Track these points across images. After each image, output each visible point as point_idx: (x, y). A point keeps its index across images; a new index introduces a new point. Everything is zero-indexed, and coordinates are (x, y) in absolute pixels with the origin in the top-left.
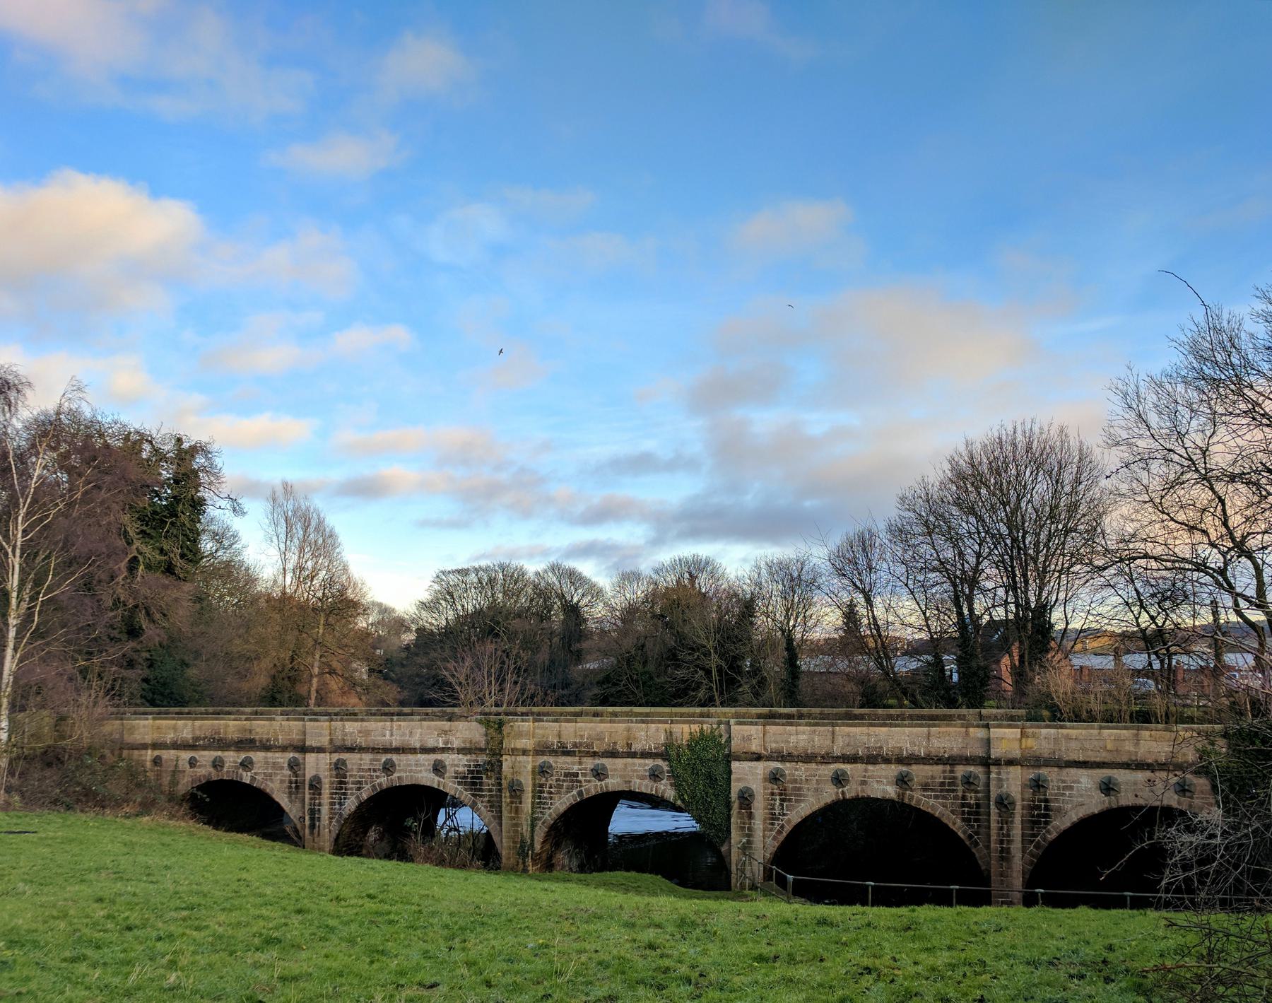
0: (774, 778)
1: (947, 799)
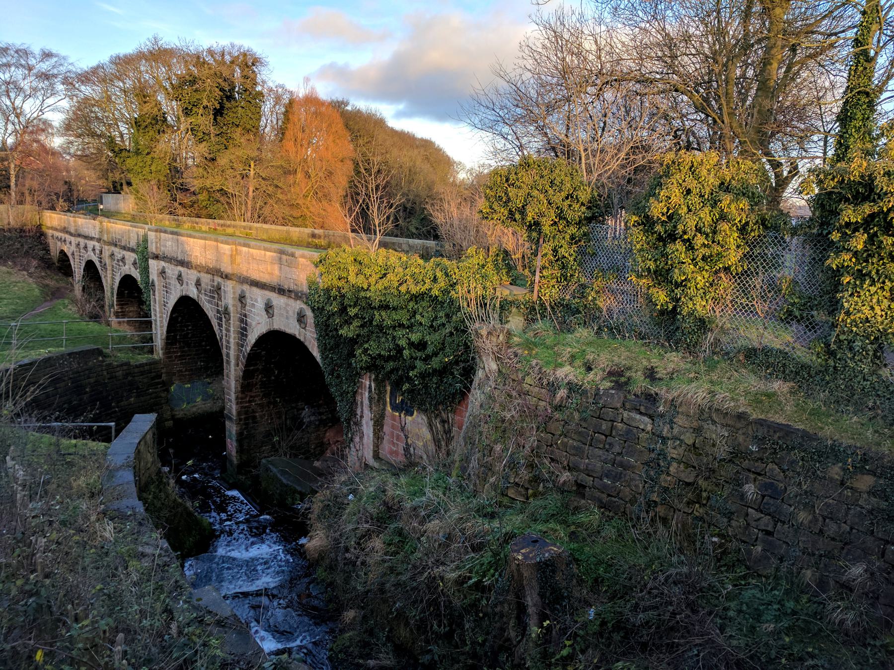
0: (163, 272)
1: (212, 304)
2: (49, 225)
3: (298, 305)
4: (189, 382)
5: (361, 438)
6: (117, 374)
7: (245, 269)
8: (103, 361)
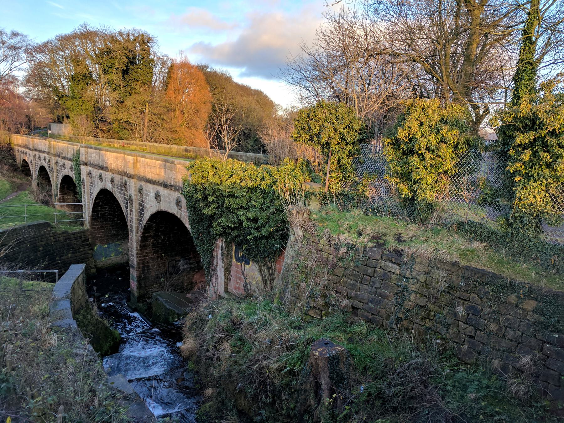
0: (90, 174)
2: (16, 143)
3: (176, 195)
4: (106, 244)
5: (217, 279)
6: (60, 239)
7: (142, 172)
8: (51, 231)
